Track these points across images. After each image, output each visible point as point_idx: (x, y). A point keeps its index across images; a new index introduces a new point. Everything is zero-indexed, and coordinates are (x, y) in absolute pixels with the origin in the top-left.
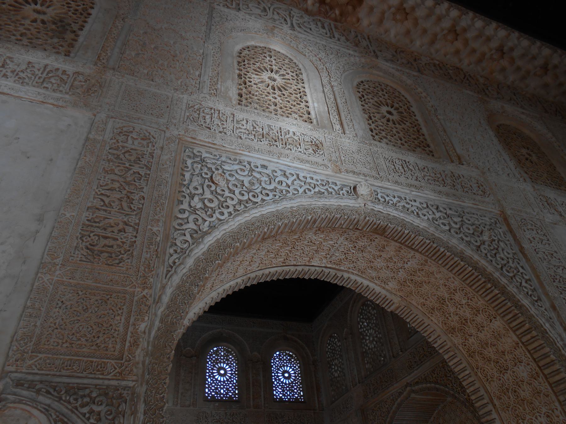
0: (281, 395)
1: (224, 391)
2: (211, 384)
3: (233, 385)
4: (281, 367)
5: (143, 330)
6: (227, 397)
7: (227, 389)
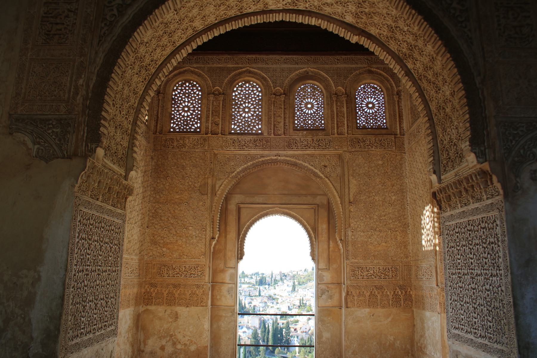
1: (312, 122)
2: (300, 116)
4: (365, 99)
5: (81, 84)
6: (314, 127)
7: (314, 120)
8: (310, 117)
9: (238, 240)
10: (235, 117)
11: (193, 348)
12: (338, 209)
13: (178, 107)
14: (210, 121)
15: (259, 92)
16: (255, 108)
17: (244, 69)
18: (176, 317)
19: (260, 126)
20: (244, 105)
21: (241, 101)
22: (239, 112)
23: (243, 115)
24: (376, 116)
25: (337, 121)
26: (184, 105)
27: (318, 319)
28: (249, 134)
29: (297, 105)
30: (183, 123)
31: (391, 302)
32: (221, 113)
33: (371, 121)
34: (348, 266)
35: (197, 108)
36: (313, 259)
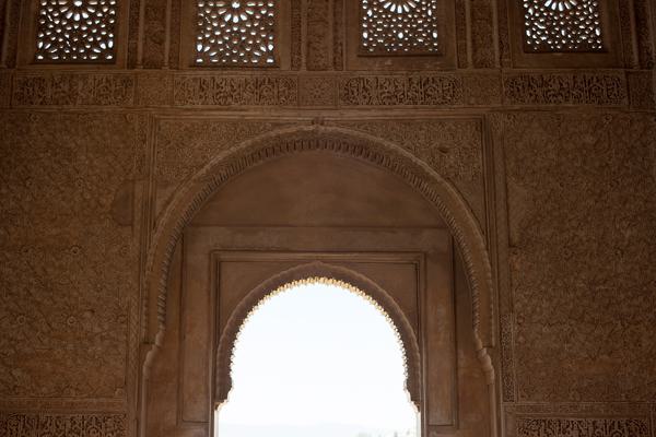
0: (544, 38)
1: (405, 35)
2: (375, 21)
6: (412, 47)
7: (411, 29)
9: (216, 347)
10: (205, 24)
12: (478, 263)
14: (141, 35)
25: (473, 33)
28: (244, 67)
30: (70, 40)
32: (168, 13)
33: (563, 32)
34: (510, 417)
36: (414, 398)
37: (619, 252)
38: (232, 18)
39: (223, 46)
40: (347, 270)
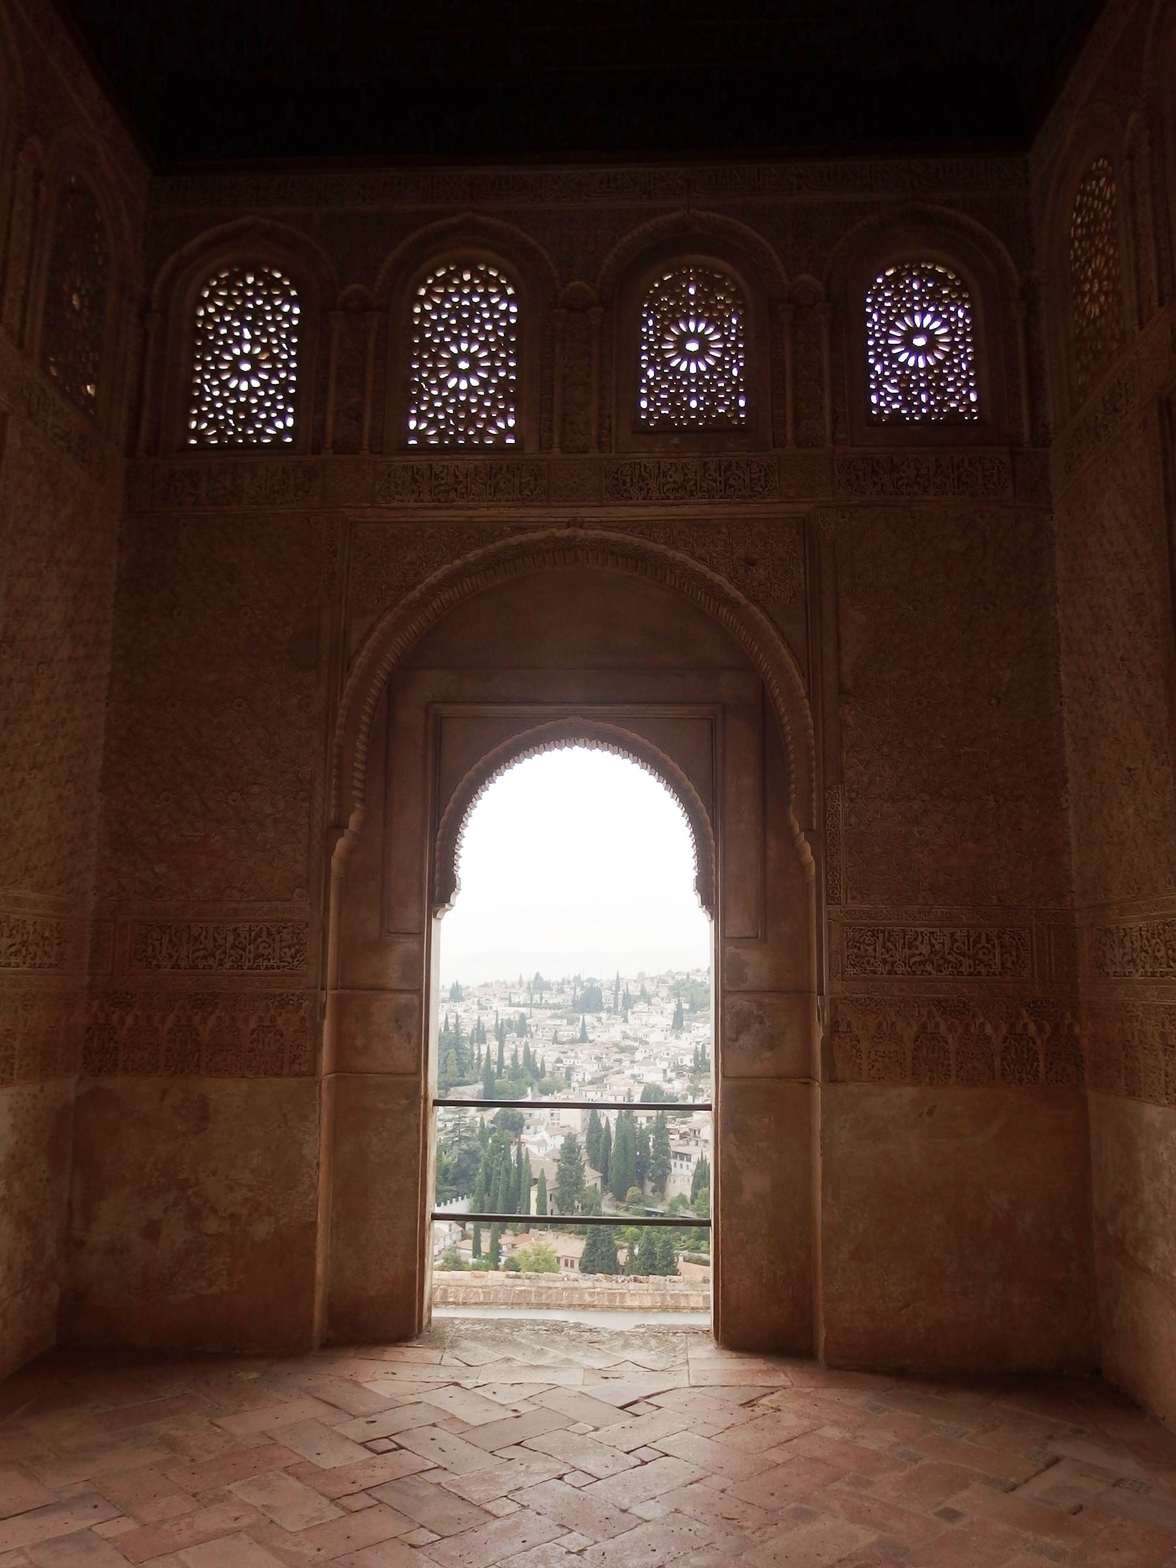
0: (895, 406)
1: (700, 403)
2: (658, 384)
3: (728, 384)
7: (709, 396)
8: (695, 385)
9: (434, 832)
10: (421, 392)
11: (262, 1230)
13: (218, 360)
15: (510, 300)
16: (492, 357)
17: (454, 220)
18: (202, 1115)
19: (511, 422)
20: (454, 349)
21: (441, 335)
22: (435, 372)
23: (452, 383)
24: (942, 377)
26: (237, 351)
27: (725, 1124)
28: (469, 448)
29: (647, 342)
31: (997, 1065)
33: (924, 398)
35: (286, 363)
37: (994, 702)
38: (458, 384)
39: (446, 421)
40: (610, 726)
